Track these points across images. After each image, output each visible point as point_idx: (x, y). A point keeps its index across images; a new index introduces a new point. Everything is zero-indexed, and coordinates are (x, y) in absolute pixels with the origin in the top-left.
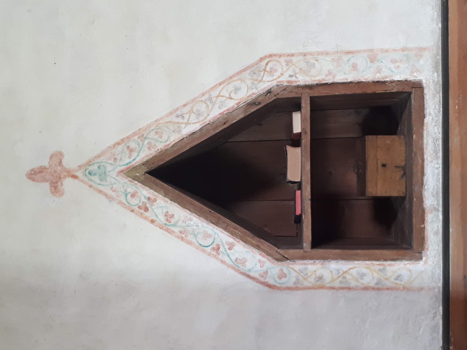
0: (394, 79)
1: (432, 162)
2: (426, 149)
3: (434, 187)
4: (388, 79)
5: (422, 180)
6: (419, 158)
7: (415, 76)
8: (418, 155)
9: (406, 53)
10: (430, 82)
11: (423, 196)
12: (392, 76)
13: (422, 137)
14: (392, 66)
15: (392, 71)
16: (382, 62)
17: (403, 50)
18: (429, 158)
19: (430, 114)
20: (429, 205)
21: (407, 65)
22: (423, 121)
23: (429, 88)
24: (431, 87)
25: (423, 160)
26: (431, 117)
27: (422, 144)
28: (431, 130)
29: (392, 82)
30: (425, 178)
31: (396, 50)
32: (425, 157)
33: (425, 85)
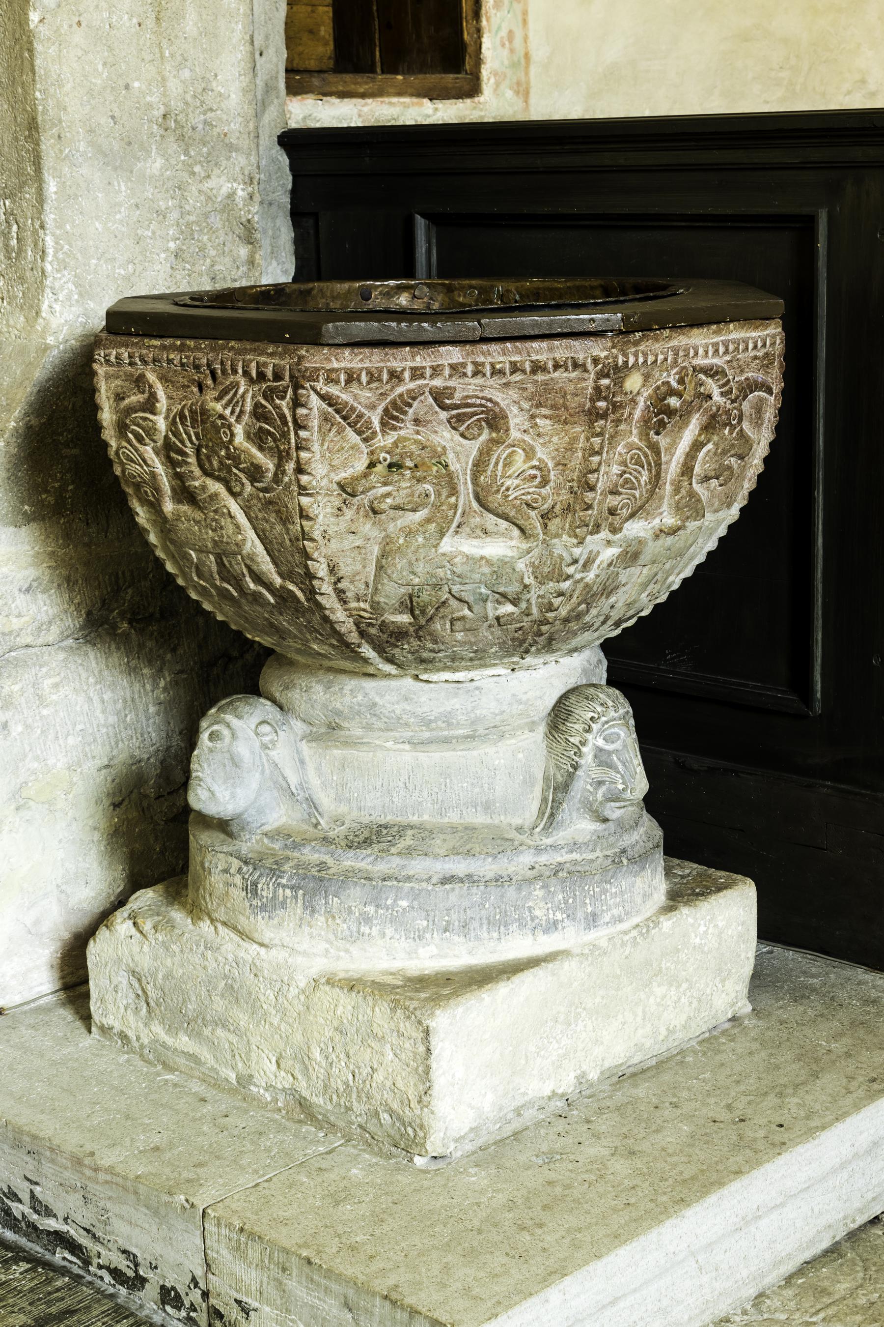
0: (485, 36)
1: (360, 116)
2: (382, 102)
3: (318, 121)
4: (484, 23)
5: (330, 94)
6: (367, 87)
7: (489, 79)
8: (371, 85)
9: (523, 61)
10: (481, 110)
11: (305, 96)
12: (490, 31)
13: (400, 94)
14: (504, 33)
15: (497, 32)
16: (509, 12)
17: (527, 56)
18: (366, 109)
19: (436, 109)
20: (290, 108)
21: (506, 62)
22: (425, 96)
23: (475, 108)
24: (474, 112)
25: (363, 96)
26: (430, 112)
27: (389, 95)
28: (411, 115)
29: (479, 31)
30: (334, 100)
31: (526, 42)
32: (369, 101)
33: (476, 99)
